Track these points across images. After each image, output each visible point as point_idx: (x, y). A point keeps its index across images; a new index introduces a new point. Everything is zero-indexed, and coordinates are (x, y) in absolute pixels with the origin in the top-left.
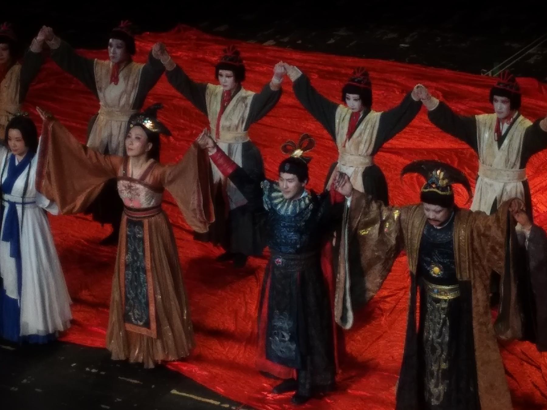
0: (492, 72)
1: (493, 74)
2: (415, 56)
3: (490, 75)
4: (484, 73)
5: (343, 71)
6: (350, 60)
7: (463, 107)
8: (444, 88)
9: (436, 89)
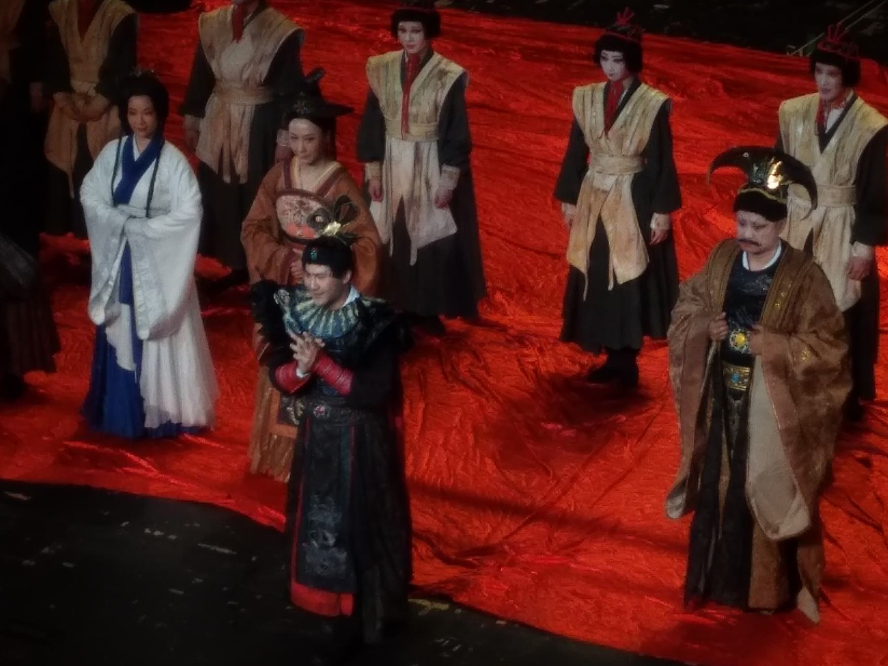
0: (803, 49)
1: (805, 53)
2: (678, 23)
3: (801, 55)
4: (791, 51)
5: (562, 48)
6: (573, 30)
7: (756, 106)
8: (726, 76)
9: (714, 77)
